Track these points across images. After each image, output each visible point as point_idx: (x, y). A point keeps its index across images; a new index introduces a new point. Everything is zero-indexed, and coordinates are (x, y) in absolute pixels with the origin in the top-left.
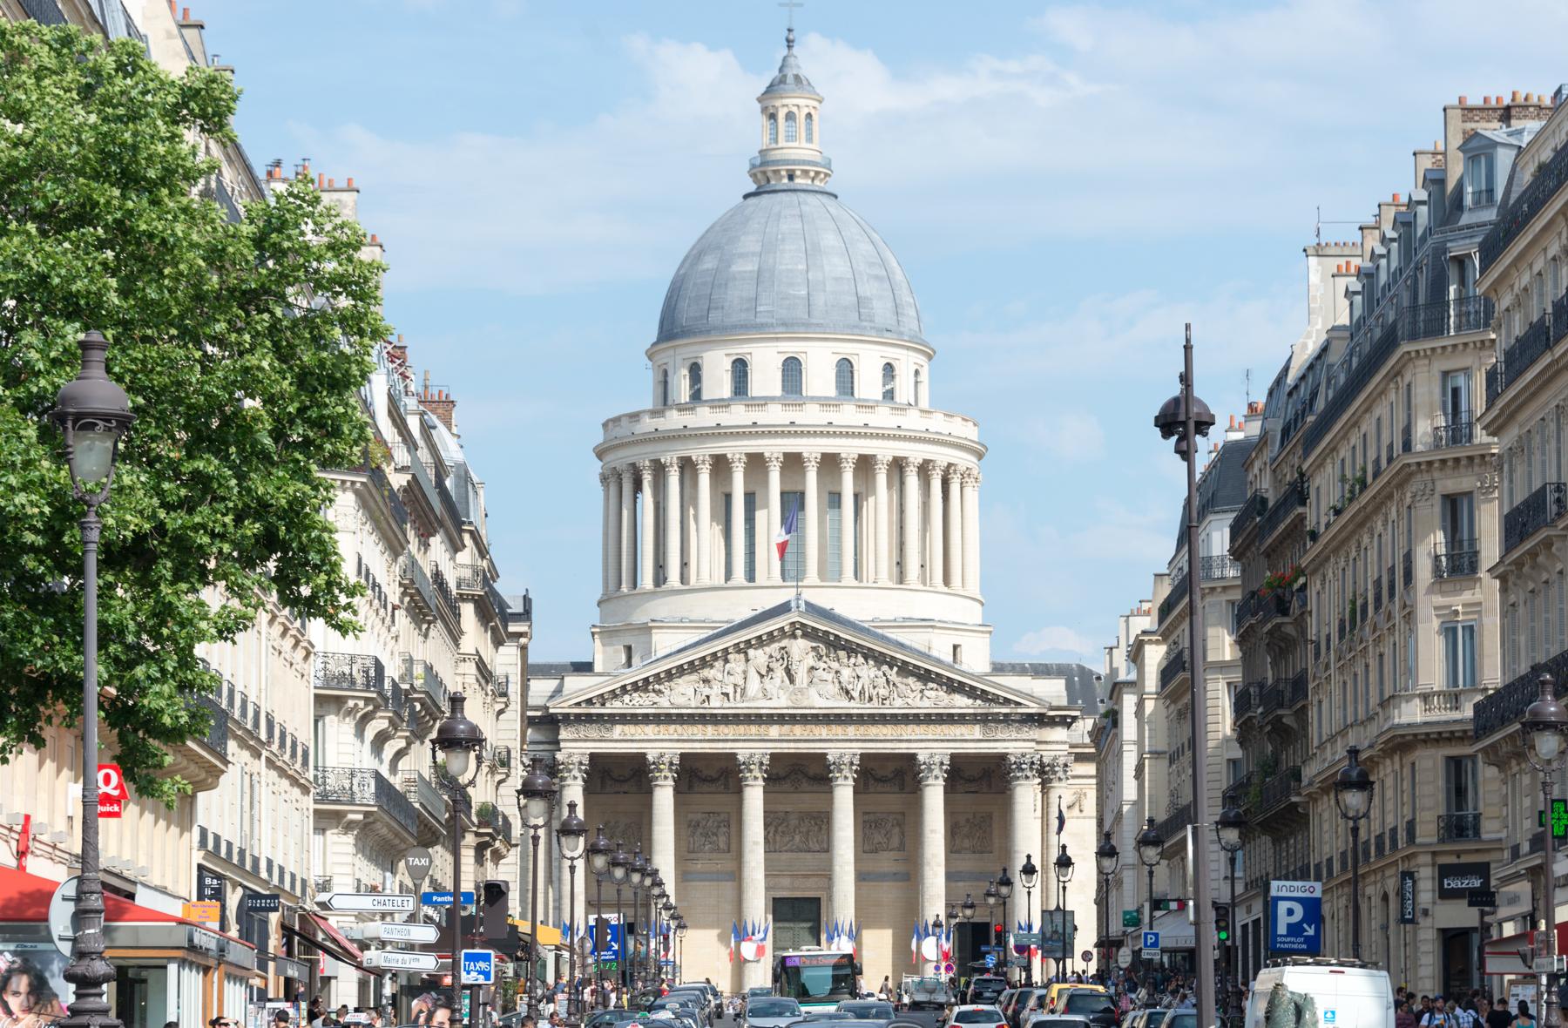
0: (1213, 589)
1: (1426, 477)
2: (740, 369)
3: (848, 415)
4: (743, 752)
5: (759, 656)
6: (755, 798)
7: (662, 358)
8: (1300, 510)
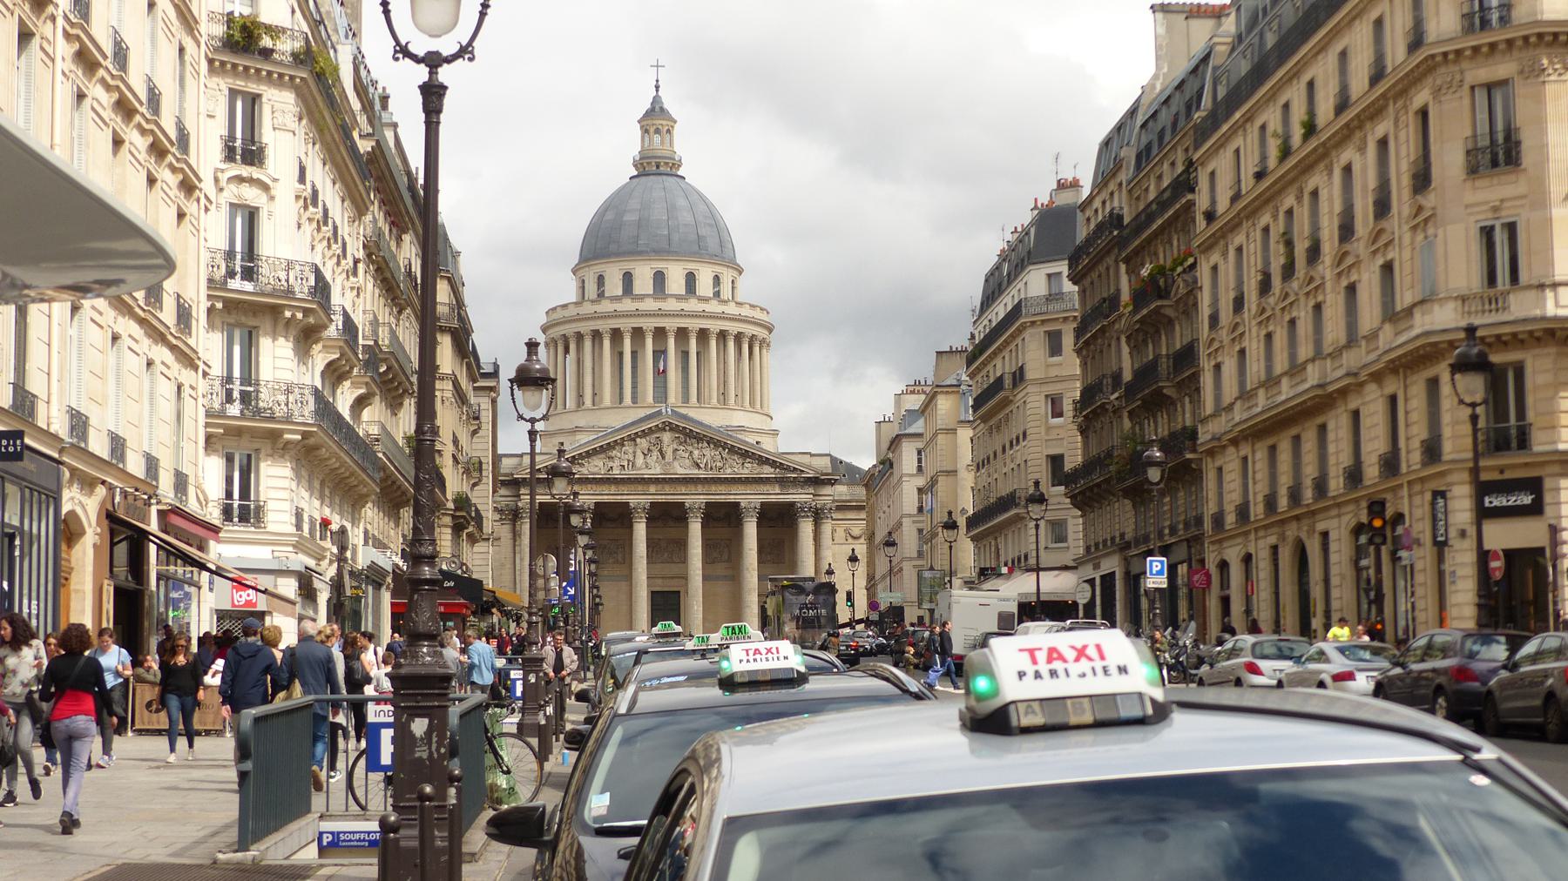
0: (1033, 323)
1: (1454, 68)
2: (628, 278)
3: (692, 305)
4: (633, 500)
5: (643, 443)
6: (640, 530)
7: (580, 273)
8: (1190, 197)
